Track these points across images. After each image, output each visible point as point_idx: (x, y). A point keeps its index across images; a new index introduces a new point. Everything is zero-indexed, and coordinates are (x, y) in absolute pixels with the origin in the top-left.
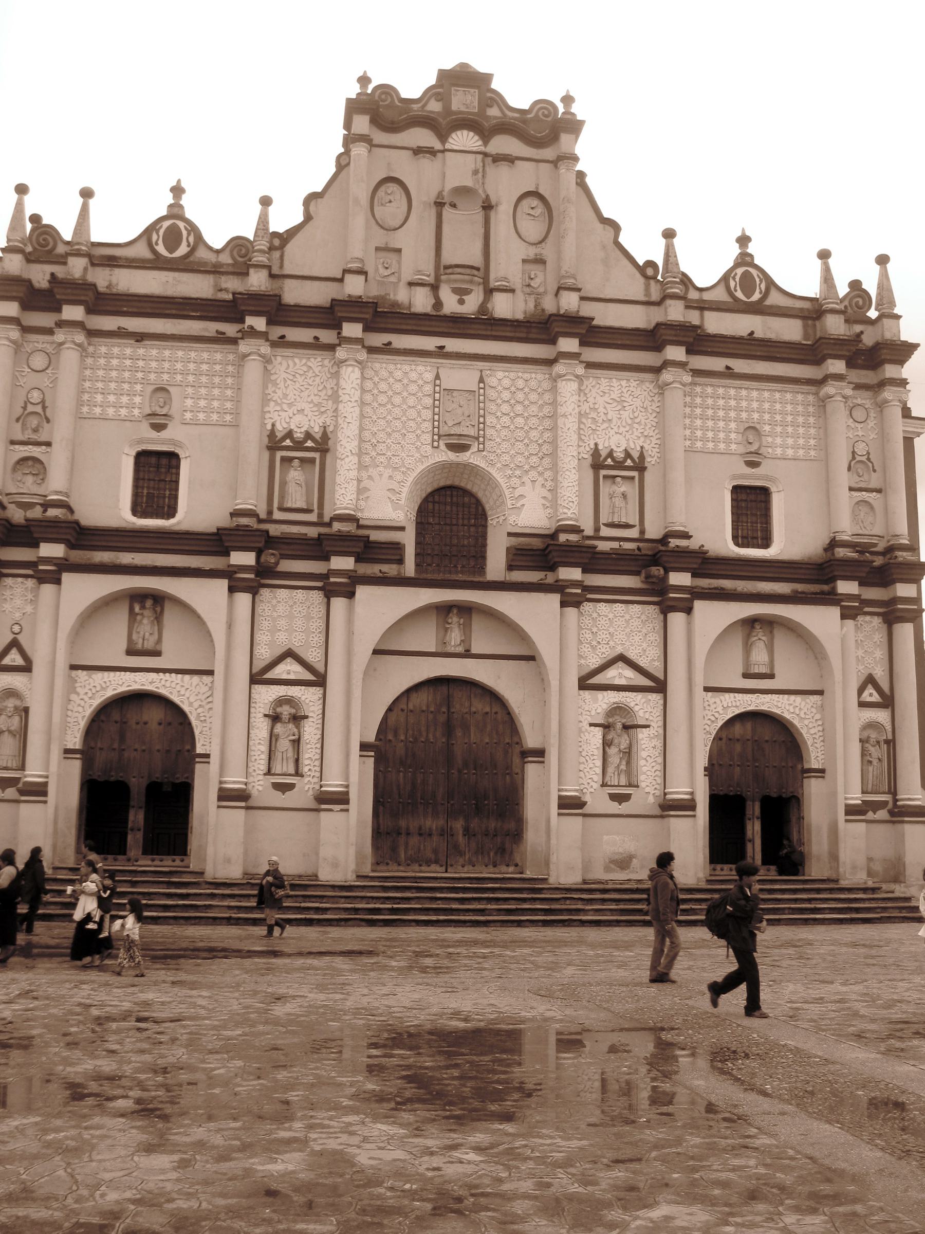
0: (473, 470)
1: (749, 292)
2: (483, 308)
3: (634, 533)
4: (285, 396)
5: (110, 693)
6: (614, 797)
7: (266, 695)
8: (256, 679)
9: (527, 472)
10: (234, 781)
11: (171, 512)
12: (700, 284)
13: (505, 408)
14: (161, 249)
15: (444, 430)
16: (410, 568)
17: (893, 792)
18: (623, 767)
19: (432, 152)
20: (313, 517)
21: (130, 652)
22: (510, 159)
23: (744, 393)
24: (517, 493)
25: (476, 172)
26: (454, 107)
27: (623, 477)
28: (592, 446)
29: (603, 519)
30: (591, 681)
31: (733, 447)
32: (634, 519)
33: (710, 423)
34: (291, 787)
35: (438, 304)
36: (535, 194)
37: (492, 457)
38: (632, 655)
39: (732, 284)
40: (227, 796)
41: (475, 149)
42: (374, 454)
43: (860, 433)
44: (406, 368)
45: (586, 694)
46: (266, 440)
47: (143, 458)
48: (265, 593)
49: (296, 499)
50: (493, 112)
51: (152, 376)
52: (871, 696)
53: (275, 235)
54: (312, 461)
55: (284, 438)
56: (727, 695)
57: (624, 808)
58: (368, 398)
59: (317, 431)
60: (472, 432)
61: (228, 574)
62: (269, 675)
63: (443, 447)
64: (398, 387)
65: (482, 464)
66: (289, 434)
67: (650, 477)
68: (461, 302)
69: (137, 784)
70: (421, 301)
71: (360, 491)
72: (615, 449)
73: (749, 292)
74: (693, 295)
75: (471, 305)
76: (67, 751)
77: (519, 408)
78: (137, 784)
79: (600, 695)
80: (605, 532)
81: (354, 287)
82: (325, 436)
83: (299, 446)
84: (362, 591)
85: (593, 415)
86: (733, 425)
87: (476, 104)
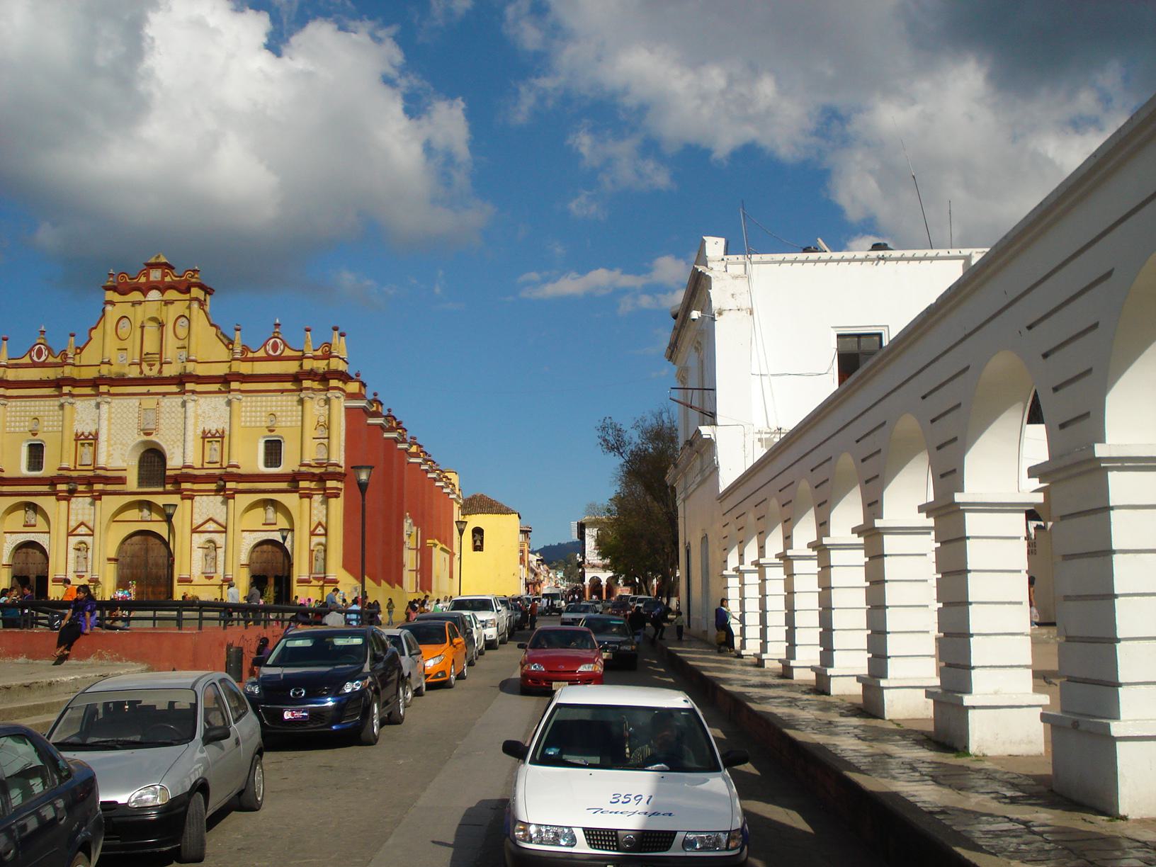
0: (157, 444)
1: (275, 351)
2: (160, 371)
3: (218, 465)
4: (82, 417)
5: (19, 542)
6: (207, 577)
7: (73, 541)
8: (69, 534)
9: (175, 442)
10: (61, 575)
11: (40, 468)
12: (252, 350)
13: (167, 415)
14: (35, 358)
15: (142, 427)
16: (132, 483)
17: (325, 573)
18: (213, 564)
19: (140, 303)
20: (91, 468)
21: (25, 526)
22: (172, 302)
23: (269, 398)
24: (171, 452)
25: (158, 309)
26: (152, 279)
27: (216, 441)
28: (202, 428)
29: (207, 459)
30: (198, 530)
31: (263, 423)
32: (218, 459)
33: (253, 414)
34: (83, 576)
35: (141, 372)
36: (183, 316)
37: (162, 437)
38: (216, 518)
39: (267, 347)
40: (55, 580)
41: (157, 299)
42: (115, 439)
43: (322, 412)
44: (128, 401)
45: (195, 535)
46: (74, 437)
47: (31, 446)
48: (73, 500)
49: (88, 460)
50: (168, 279)
51: (32, 413)
52: (320, 530)
53: (77, 348)
54: (92, 443)
55: (81, 435)
56: (255, 533)
57: (211, 582)
58: (113, 415)
59: (93, 432)
60: (153, 427)
61: (54, 493)
62: (74, 533)
63: (142, 434)
64: (125, 410)
65: (157, 440)
66: (83, 434)
67: (226, 440)
68: (151, 370)
69: (33, 577)
70: (133, 373)
71: (110, 456)
72: (211, 428)
73: (275, 351)
74: (250, 355)
75: (154, 373)
76: (4, 565)
77: (173, 415)
78: (33, 577)
79: (202, 535)
80: (206, 465)
81: (105, 370)
82: (97, 434)
83: (87, 438)
84: (103, 497)
85: (203, 415)
86: (263, 414)
87: (160, 276)
